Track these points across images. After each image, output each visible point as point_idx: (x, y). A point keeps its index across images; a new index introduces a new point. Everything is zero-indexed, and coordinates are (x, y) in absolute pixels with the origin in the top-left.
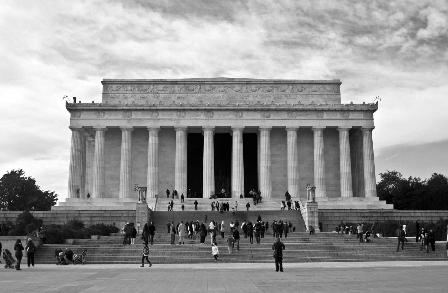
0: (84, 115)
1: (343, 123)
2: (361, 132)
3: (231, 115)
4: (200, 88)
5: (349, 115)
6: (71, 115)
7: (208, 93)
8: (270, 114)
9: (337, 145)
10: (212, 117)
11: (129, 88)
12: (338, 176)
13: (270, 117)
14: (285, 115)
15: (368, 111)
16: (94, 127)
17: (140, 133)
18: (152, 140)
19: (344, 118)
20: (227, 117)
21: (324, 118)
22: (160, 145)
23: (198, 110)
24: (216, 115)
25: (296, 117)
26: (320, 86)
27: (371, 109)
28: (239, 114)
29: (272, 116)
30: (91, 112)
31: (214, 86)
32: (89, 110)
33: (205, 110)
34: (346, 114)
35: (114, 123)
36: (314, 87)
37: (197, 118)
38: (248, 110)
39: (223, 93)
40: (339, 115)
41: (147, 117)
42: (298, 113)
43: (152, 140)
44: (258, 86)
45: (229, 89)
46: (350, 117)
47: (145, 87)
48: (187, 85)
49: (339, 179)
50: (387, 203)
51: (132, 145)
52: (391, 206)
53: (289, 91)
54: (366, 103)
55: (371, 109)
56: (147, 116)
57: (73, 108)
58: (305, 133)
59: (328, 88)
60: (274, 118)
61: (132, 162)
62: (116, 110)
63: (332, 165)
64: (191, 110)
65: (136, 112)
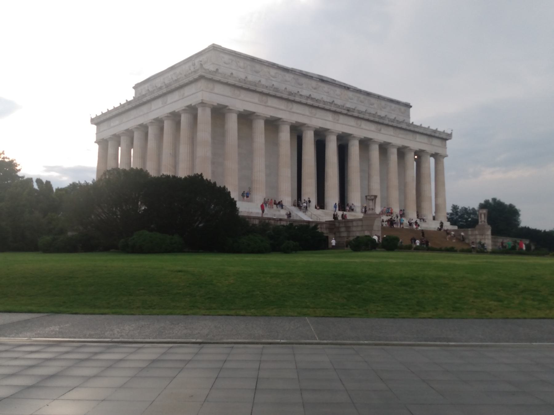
7: (315, 91)
10: (338, 120)
13: (380, 130)
14: (391, 131)
16: (231, 108)
17: (272, 124)
24: (342, 119)
27: (448, 138)
28: (359, 122)
32: (227, 84)
33: (335, 112)
35: (251, 108)
36: (393, 106)
40: (425, 139)
41: (282, 107)
42: (402, 132)
54: (446, 132)
56: (282, 105)
59: (403, 108)
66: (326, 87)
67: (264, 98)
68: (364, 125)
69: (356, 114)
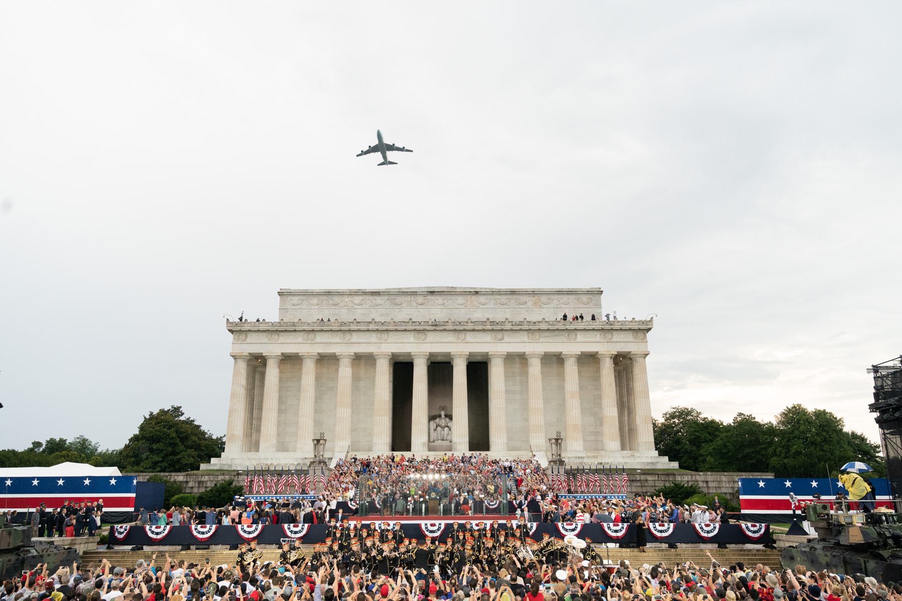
0: (252, 338)
1: (606, 347)
2: (630, 359)
3: (450, 337)
6: (234, 338)
9: (597, 378)
10: (425, 339)
11: (315, 301)
12: (600, 421)
13: (502, 339)
14: (524, 337)
15: (639, 329)
17: (326, 360)
18: (345, 371)
20: (445, 340)
22: (356, 378)
23: (405, 330)
24: (431, 337)
26: (573, 297)
28: (462, 335)
29: (506, 339)
30: (261, 334)
31: (429, 297)
34: (609, 335)
35: (291, 349)
36: (565, 298)
37: (405, 341)
38: (474, 330)
40: (598, 336)
41: (337, 340)
43: (345, 371)
44: (489, 297)
45: (450, 302)
46: (614, 339)
47: (336, 299)
48: (393, 297)
49: (601, 424)
50: (670, 460)
51: (318, 378)
52: (675, 465)
53: (530, 304)
55: (642, 329)
56: (337, 338)
57: (238, 329)
59: (584, 298)
60: (509, 340)
61: (316, 402)
62: (295, 331)
63: (592, 406)
64: (396, 330)
65: (322, 333)
66: (439, 300)
67: (311, 335)
68: (469, 337)
69: (452, 328)
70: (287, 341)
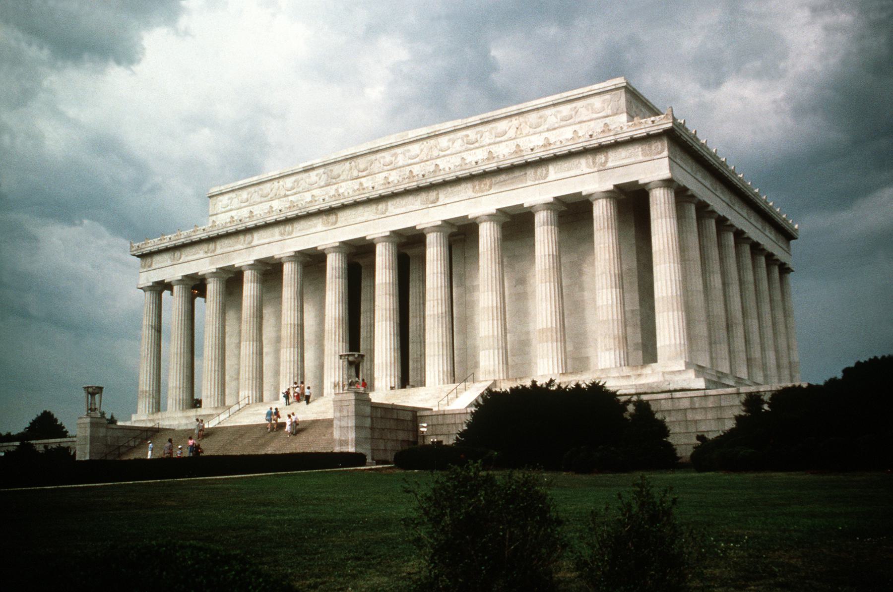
0: (158, 261)
4: (351, 169)
5: (606, 162)
8: (438, 194)
10: (336, 222)
13: (437, 199)
19: (596, 169)
21: (548, 179)
25: (490, 187)
34: (601, 158)
38: (394, 195)
39: (389, 167)
40: (583, 164)
44: (452, 136)
48: (330, 167)
58: (516, 225)
70: (190, 258)
